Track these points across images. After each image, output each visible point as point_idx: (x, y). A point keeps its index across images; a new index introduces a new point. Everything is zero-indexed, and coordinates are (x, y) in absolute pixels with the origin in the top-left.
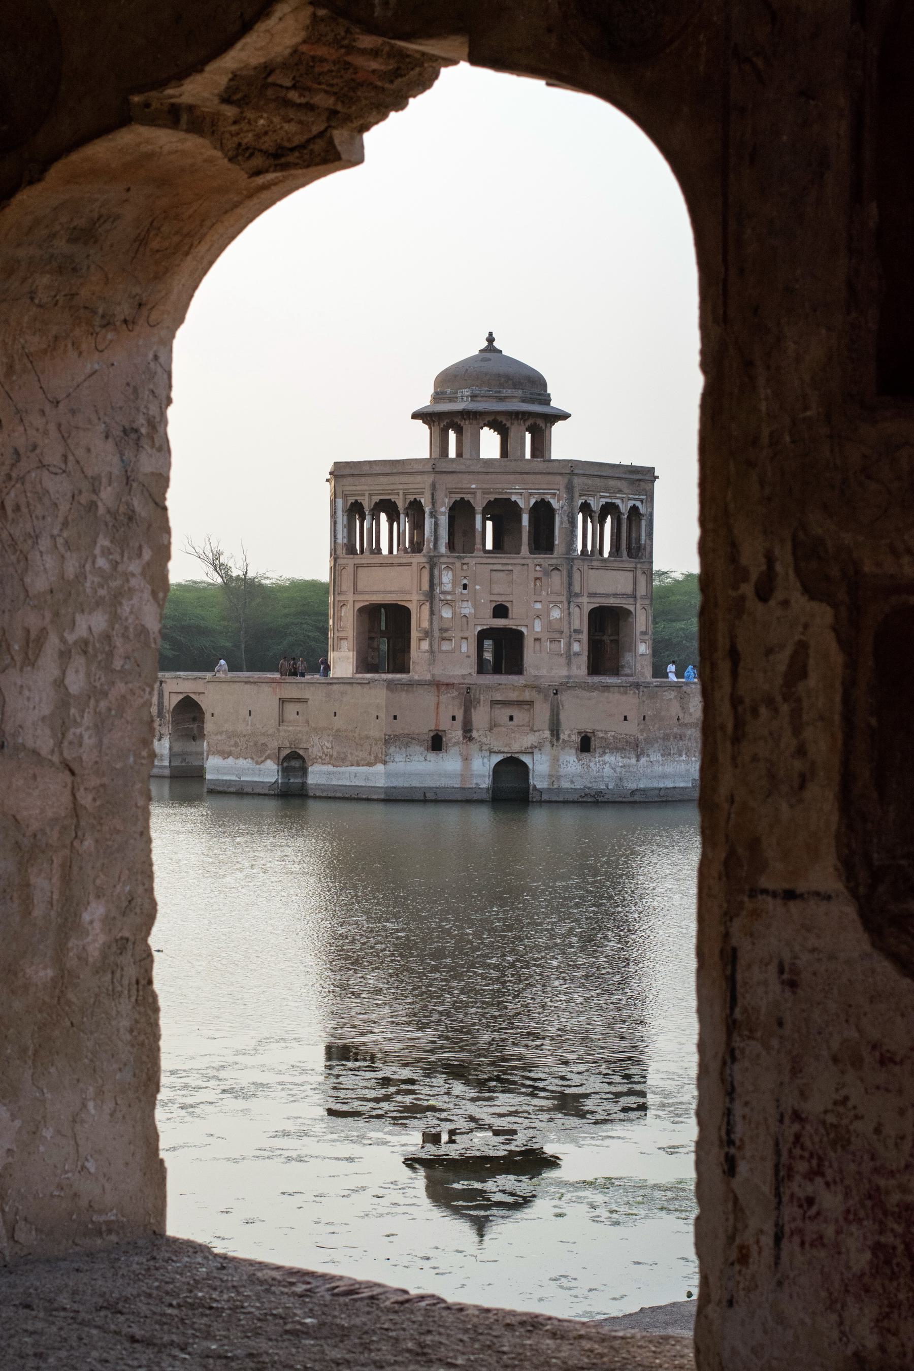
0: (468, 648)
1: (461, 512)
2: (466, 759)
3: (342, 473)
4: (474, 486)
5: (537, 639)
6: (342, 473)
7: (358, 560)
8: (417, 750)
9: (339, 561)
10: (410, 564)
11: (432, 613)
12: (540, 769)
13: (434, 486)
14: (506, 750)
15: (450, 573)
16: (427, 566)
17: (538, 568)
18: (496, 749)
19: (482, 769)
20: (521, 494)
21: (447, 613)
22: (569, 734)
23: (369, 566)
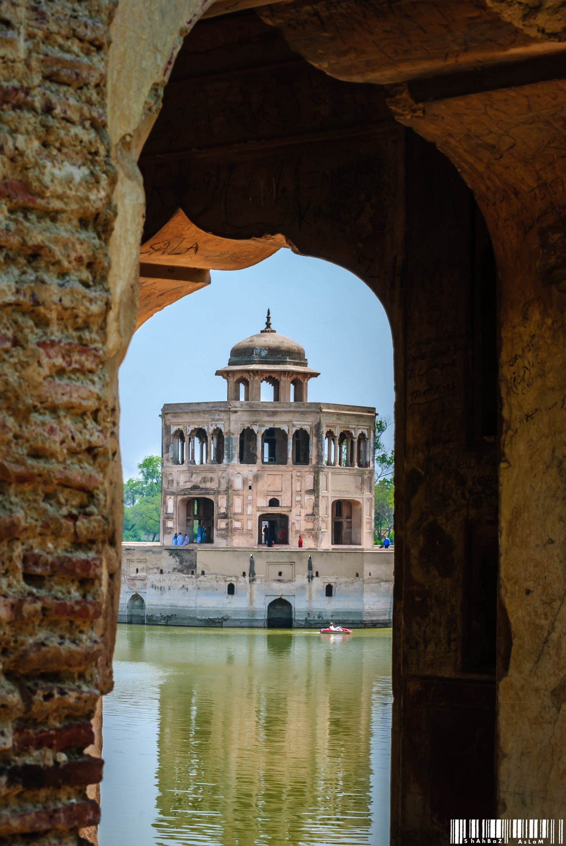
1: (247, 436)
3: (169, 411)
6: (169, 411)
12: (300, 606)
19: (261, 605)
22: (319, 584)
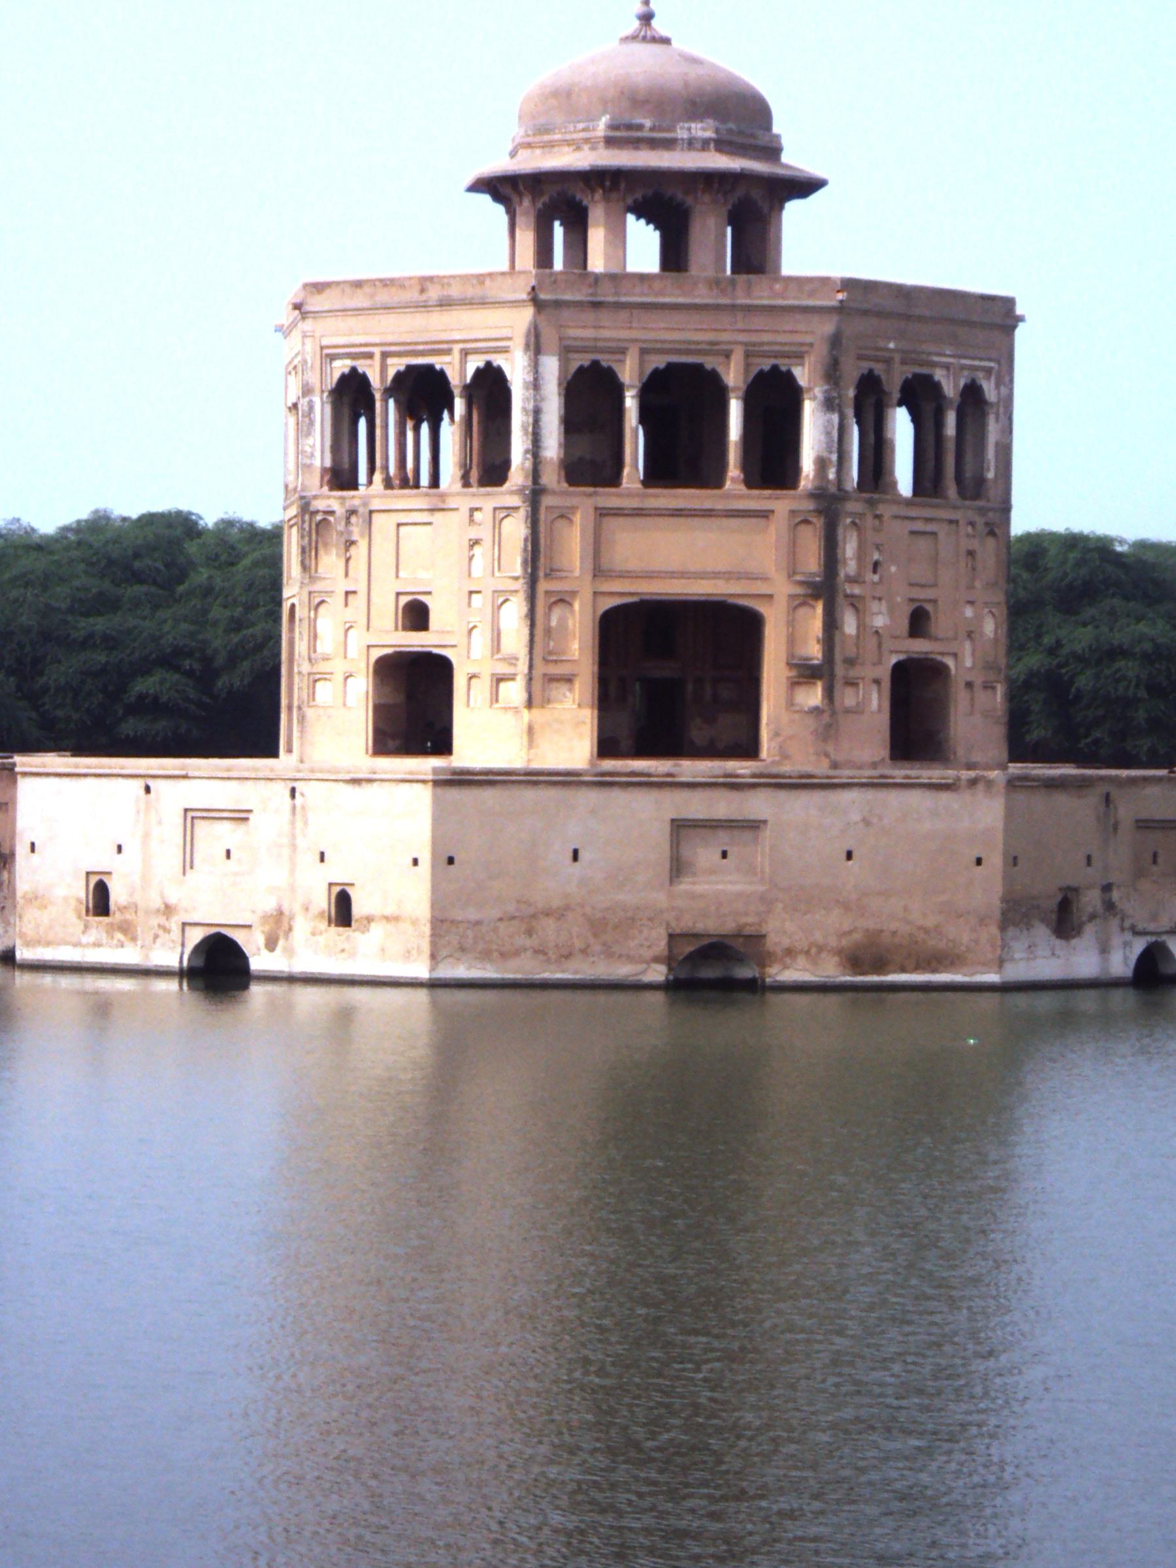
0: (873, 704)
2: (1104, 950)
4: (892, 345)
5: (969, 685)
7: (608, 498)
8: (1042, 933)
9: (547, 501)
10: (765, 515)
11: (831, 624)
13: (836, 341)
14: (1152, 927)
15: (855, 534)
16: (819, 522)
17: (970, 529)
18: (1140, 927)
20: (947, 367)
21: (849, 625)
23: (638, 513)
